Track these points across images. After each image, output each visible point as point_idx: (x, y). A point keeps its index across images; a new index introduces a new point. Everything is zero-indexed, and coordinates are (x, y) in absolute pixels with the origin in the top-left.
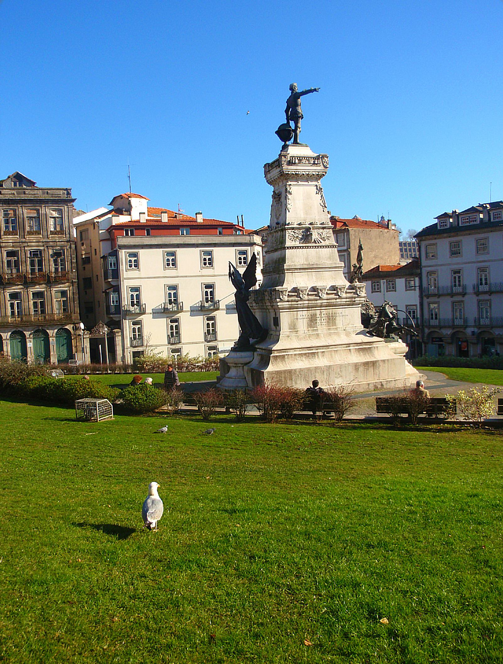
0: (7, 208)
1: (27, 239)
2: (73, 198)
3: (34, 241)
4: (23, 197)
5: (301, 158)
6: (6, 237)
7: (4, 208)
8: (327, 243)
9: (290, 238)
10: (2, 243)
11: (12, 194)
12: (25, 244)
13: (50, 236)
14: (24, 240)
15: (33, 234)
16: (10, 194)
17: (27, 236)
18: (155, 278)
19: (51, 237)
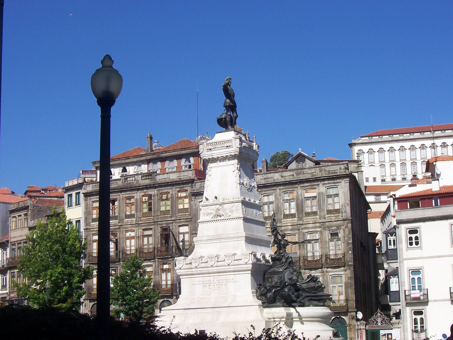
0: (287, 190)
1: (305, 220)
2: (363, 170)
3: (311, 222)
4: (302, 177)
5: (223, 142)
6: (285, 220)
7: (284, 190)
8: (235, 215)
9: (204, 214)
10: (281, 226)
11: (291, 175)
12: (303, 226)
13: (327, 216)
14: (301, 222)
15: (309, 216)
16: (289, 176)
17: (305, 218)
18: (439, 257)
19: (328, 217)
